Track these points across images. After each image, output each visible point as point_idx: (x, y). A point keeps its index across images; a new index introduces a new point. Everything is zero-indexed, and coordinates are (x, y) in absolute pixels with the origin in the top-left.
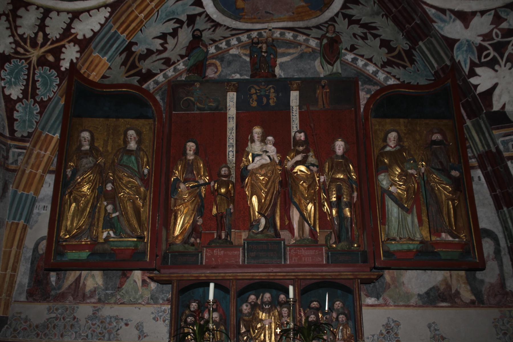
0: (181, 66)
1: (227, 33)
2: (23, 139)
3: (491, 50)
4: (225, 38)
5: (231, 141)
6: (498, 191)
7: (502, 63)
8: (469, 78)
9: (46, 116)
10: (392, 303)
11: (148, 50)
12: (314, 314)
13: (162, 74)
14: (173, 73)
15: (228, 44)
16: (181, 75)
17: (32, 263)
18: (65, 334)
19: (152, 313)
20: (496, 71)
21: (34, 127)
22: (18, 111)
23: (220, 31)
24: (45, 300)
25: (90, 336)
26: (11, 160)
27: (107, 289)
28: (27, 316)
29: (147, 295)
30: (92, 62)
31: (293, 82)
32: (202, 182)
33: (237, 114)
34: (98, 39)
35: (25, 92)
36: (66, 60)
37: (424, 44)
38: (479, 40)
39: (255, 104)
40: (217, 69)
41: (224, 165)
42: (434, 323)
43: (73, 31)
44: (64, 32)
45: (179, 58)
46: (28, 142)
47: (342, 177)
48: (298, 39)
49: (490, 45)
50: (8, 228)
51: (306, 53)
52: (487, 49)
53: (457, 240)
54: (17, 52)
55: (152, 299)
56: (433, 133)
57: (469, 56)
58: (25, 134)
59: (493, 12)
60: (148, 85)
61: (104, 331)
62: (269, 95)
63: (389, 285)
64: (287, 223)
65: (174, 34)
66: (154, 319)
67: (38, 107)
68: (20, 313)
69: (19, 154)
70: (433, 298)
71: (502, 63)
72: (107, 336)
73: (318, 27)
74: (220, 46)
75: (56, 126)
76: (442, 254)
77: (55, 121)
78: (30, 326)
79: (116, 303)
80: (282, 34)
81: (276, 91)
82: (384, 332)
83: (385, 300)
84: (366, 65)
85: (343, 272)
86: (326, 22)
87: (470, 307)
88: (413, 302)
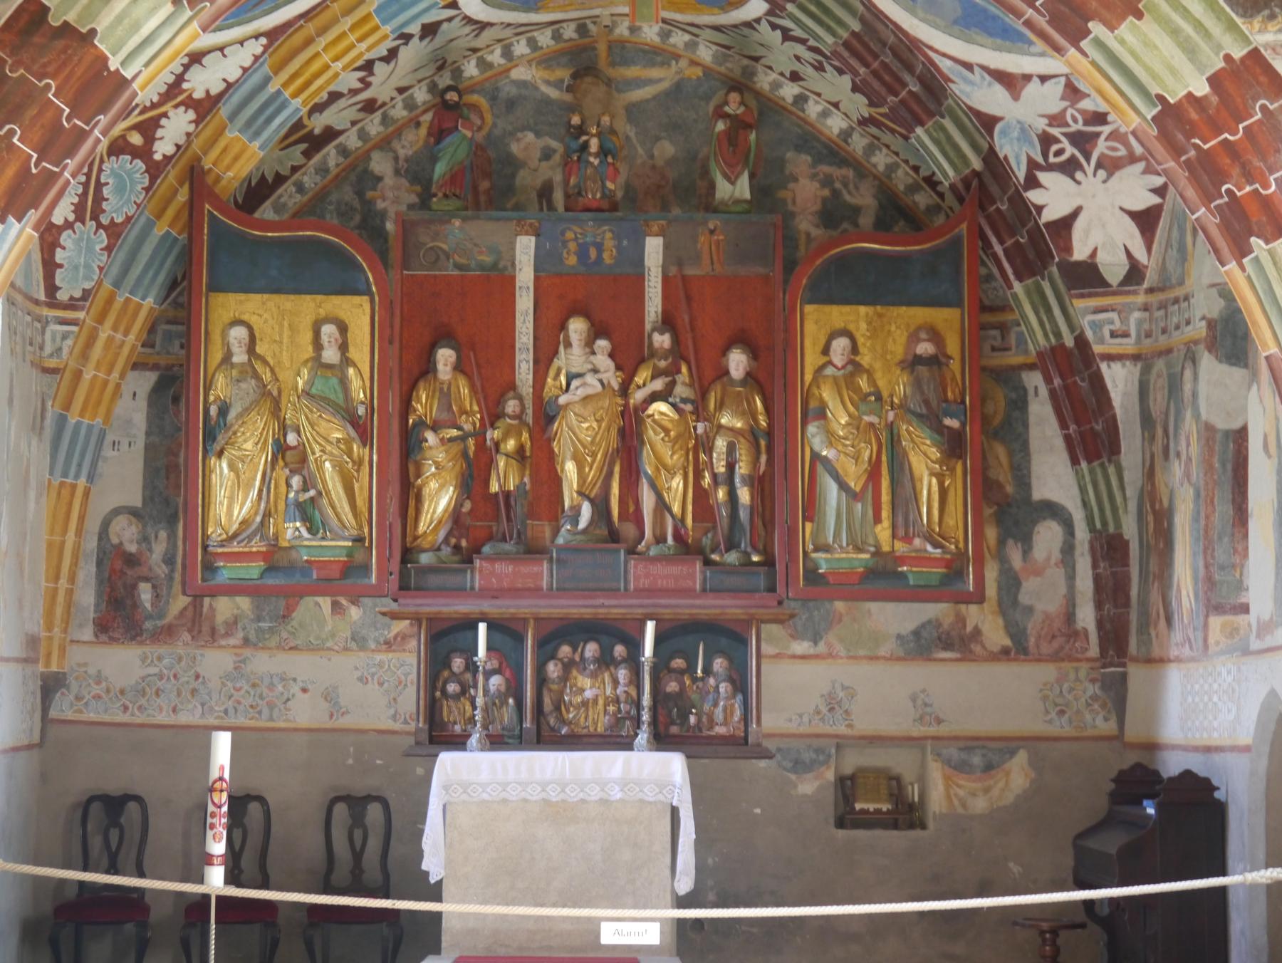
0: (399, 112)
1: (508, 32)
2: (72, 305)
3: (1065, 143)
4: (499, 41)
5: (524, 339)
6: (1073, 428)
7: (1090, 169)
8: (1026, 189)
10: (843, 653)
11: (331, 94)
12: (676, 680)
13: (356, 128)
14: (381, 129)
15: (507, 53)
16: (400, 135)
17: (99, 563)
18: (180, 706)
19: (356, 668)
20: (1079, 183)
21: (96, 278)
22: (64, 248)
23: (488, 35)
24: (133, 638)
25: (231, 711)
26: (48, 349)
27: (259, 619)
28: (99, 671)
30: (225, 150)
31: (651, 223)
32: (468, 427)
33: (537, 278)
34: (236, 98)
35: (79, 210)
36: (166, 140)
37: (927, 131)
38: (1041, 124)
39: (572, 260)
40: (482, 118)
41: (511, 394)
42: (923, 691)
43: (185, 86)
44: (168, 91)
45: (395, 94)
46: (82, 308)
47: (739, 425)
48: (672, 40)
49: (1065, 134)
50: (54, 494)
51: (689, 79)
52: (1057, 141)
53: (939, 551)
55: (353, 639)
56: (919, 340)
57: (1024, 149)
58: (78, 294)
59: (1063, 80)
60: (325, 158)
61: (260, 702)
62: (602, 244)
63: (841, 615)
64: (631, 509)
65: (392, 54)
66: (360, 679)
67: (104, 235)
68: (85, 664)
69: (65, 336)
71: (1090, 169)
72: (266, 712)
73: (717, 28)
74: (489, 58)
75: (146, 282)
76: (910, 577)
77: (145, 271)
78: (108, 691)
79: (280, 647)
81: (617, 237)
82: (824, 710)
83: (829, 645)
84: (825, 114)
86: (735, 26)
87: (999, 660)
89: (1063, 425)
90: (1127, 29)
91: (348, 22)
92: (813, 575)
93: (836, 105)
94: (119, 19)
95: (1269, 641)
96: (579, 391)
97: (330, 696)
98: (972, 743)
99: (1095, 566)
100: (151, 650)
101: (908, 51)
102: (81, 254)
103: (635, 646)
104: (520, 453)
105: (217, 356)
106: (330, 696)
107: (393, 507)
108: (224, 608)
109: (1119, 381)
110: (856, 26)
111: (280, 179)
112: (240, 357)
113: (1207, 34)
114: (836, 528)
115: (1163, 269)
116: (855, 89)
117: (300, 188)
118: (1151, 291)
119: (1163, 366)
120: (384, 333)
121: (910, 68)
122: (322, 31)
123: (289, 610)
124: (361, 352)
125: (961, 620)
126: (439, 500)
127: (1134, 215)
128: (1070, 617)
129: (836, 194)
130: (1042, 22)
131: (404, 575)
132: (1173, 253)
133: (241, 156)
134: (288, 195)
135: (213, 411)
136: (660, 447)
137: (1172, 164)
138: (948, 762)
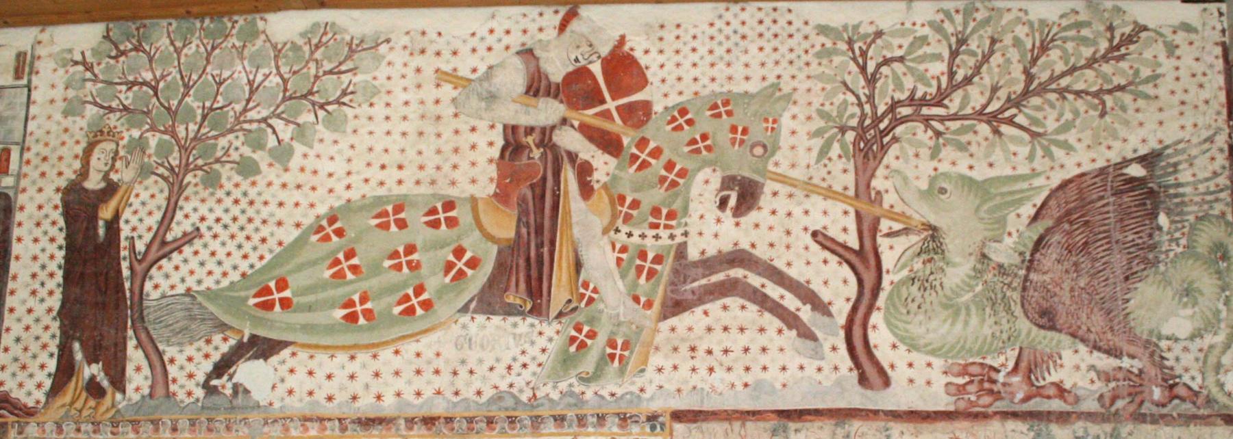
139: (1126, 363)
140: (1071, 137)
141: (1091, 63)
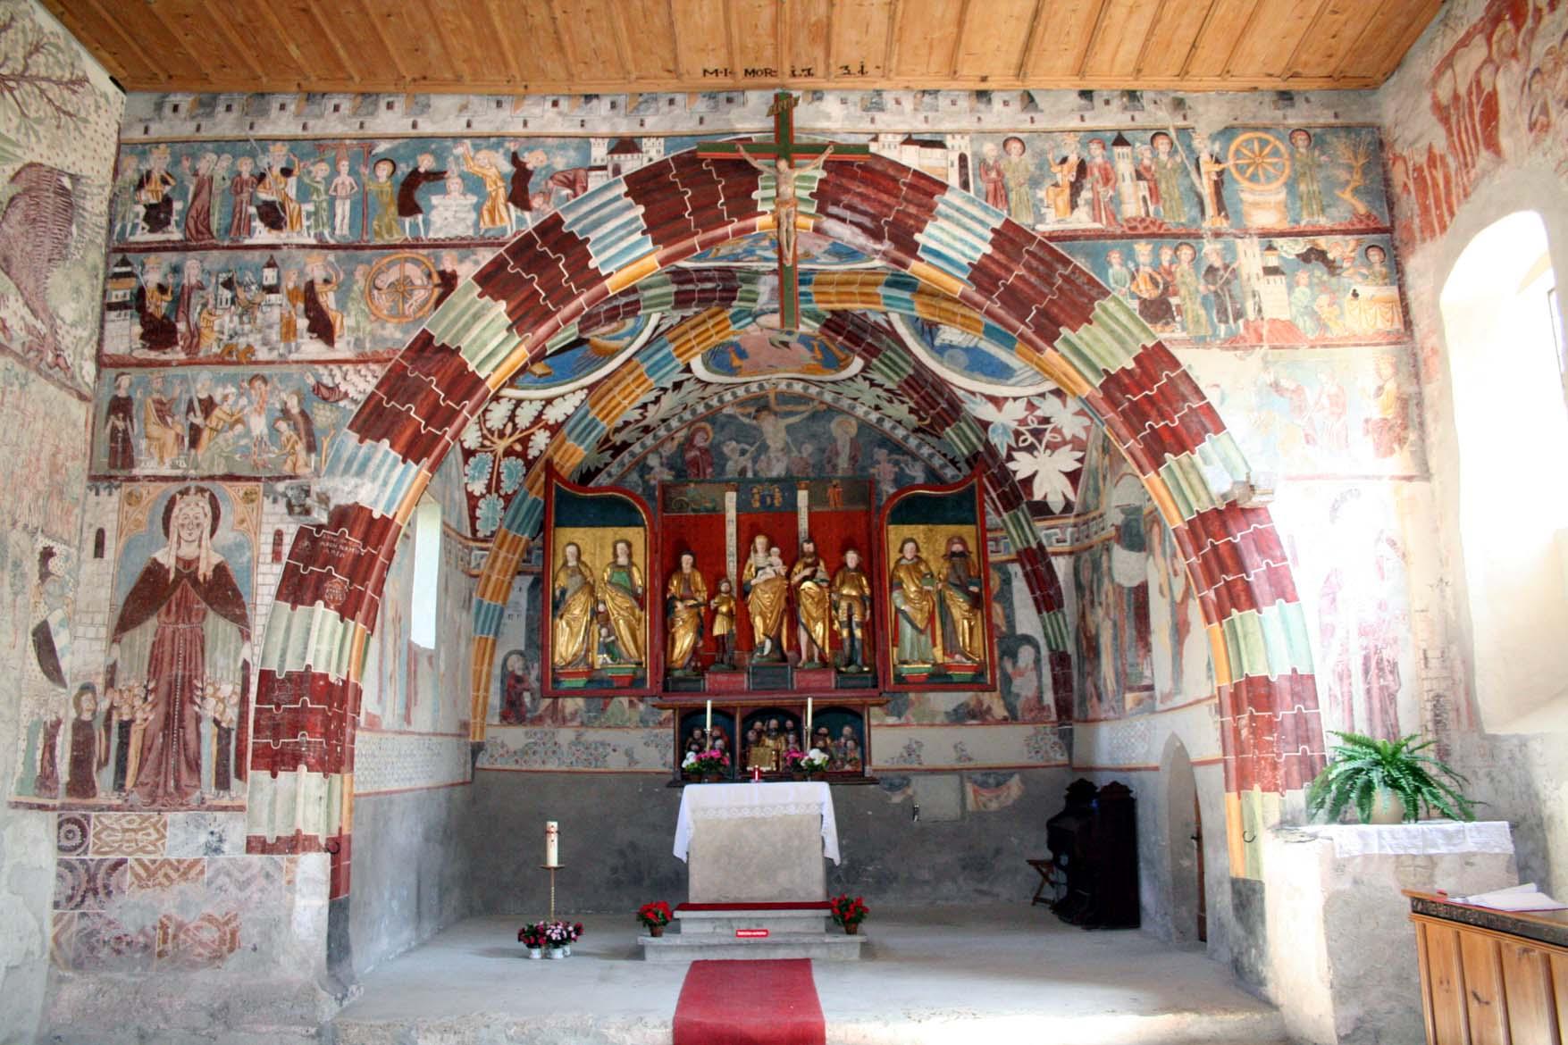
1: (720, 389)
2: (485, 540)
3: (1028, 435)
9: (511, 512)
15: (721, 400)
23: (710, 390)
26: (473, 564)
29: (636, 718)
34: (572, 423)
35: (489, 487)
38: (1014, 425)
39: (757, 505)
54: (483, 446)
65: (657, 400)
70: (961, 716)
73: (834, 382)
79: (600, 727)
80: (789, 386)
81: (782, 490)
84: (894, 428)
85: (850, 698)
88: (938, 721)
89: (1033, 592)
90: (1083, 330)
91: (631, 378)
92: (900, 679)
93: (900, 422)
94: (474, 341)
95: (1169, 704)
96: (762, 577)
97: (629, 753)
98: (988, 771)
99: (1053, 670)
100: (529, 728)
101: (940, 385)
102: (489, 510)
103: (798, 722)
104: (730, 614)
105: (560, 562)
106: (629, 753)
107: (658, 642)
108: (571, 705)
109: (1061, 566)
110: (911, 372)
111: (598, 471)
112: (572, 563)
113: (1131, 333)
114: (914, 650)
115: (1084, 503)
116: (911, 411)
117: (610, 475)
118: (1078, 516)
119: (1090, 559)
120: (653, 548)
121: (941, 394)
122: (617, 384)
123: (606, 705)
124: (639, 558)
125: (980, 703)
126: (684, 641)
127: (1068, 475)
128: (1040, 698)
129: (902, 469)
130: (1029, 333)
131: (665, 683)
132: (1091, 493)
133: (575, 454)
134: (603, 480)
135: (558, 593)
136: (808, 607)
137: (1112, 414)
138: (975, 782)
139: (39, 325)
140: (41, 129)
141: (59, 83)
